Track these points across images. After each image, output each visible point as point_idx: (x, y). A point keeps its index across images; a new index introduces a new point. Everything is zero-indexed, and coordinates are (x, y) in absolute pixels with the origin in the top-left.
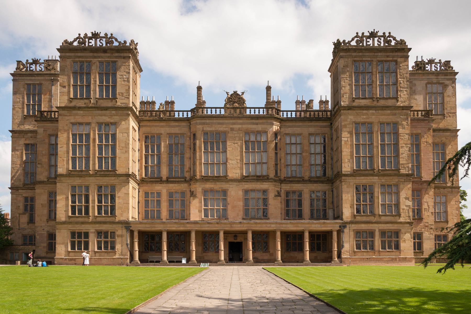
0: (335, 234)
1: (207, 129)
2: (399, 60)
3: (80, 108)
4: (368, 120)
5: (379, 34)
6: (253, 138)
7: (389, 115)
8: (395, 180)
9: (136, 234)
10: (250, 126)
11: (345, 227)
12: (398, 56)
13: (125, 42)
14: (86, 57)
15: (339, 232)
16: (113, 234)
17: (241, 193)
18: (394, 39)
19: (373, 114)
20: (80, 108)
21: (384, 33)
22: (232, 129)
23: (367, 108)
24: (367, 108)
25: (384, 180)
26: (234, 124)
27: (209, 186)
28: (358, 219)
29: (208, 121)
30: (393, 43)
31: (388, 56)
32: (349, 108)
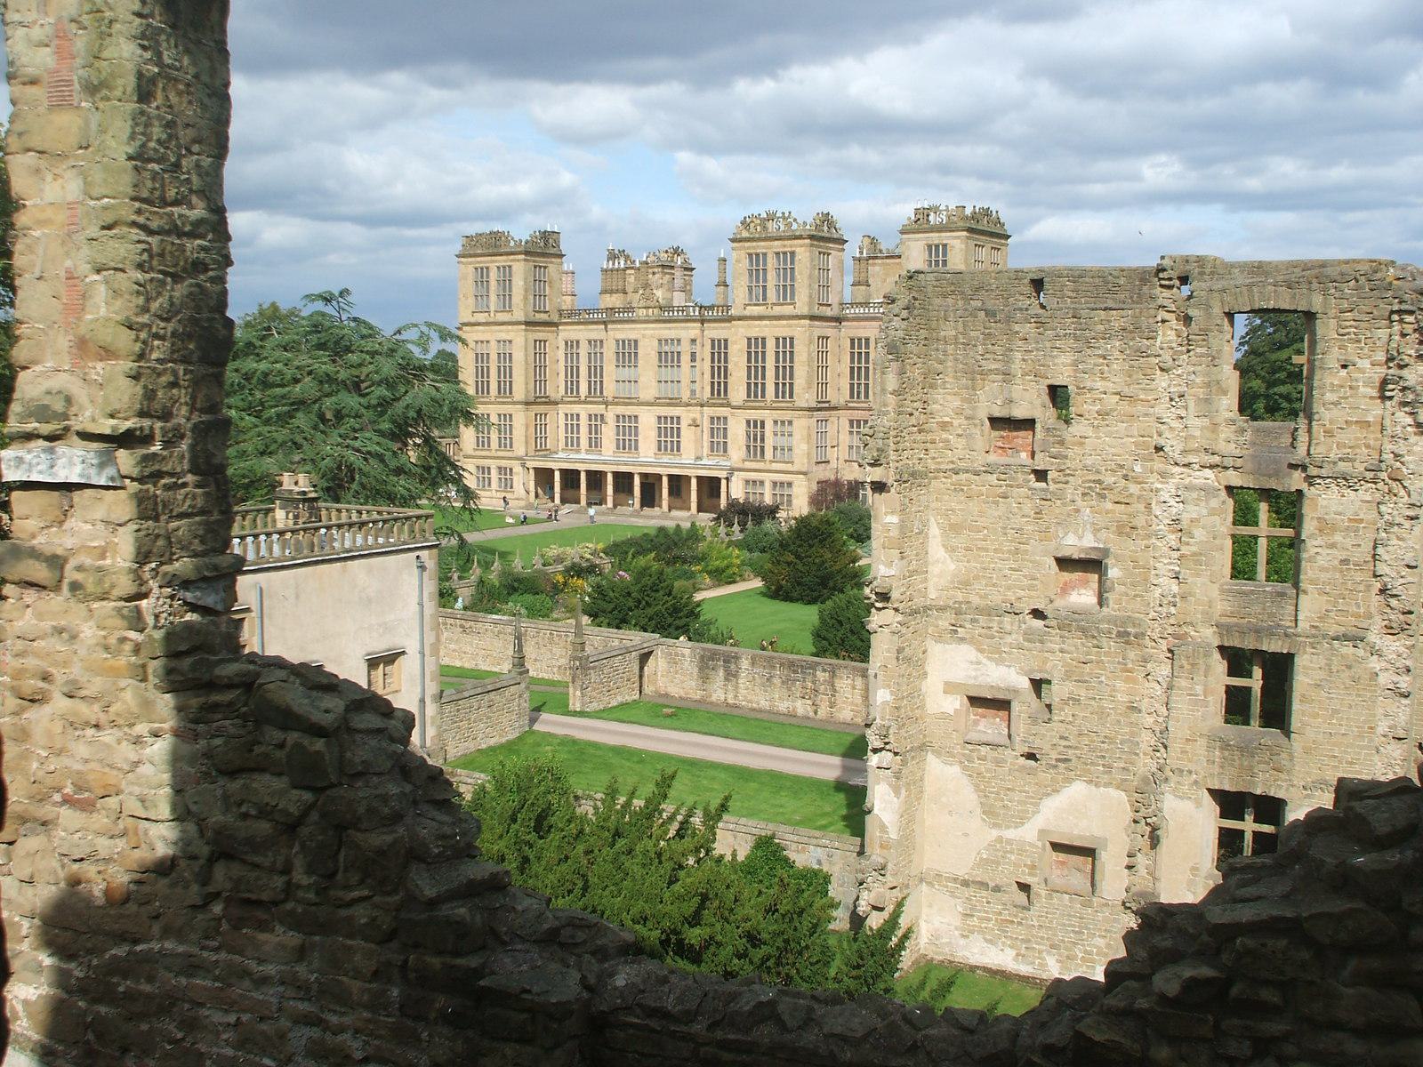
0: (724, 482)
1: (621, 336)
2: (798, 250)
3: (479, 324)
4: (762, 335)
5: (779, 214)
6: (667, 348)
7: (784, 326)
8: (787, 415)
9: (532, 472)
10: (662, 332)
11: (732, 474)
12: (796, 246)
13: (521, 241)
14: (485, 262)
15: (727, 479)
16: (511, 470)
17: (654, 420)
18: (795, 220)
19: (766, 326)
20: (479, 324)
21: (783, 213)
22: (644, 336)
23: (761, 318)
24: (761, 318)
25: (778, 415)
26: (646, 329)
27: (621, 410)
28: (748, 465)
29: (619, 326)
30: (795, 226)
31: (785, 246)
32: (740, 318)
